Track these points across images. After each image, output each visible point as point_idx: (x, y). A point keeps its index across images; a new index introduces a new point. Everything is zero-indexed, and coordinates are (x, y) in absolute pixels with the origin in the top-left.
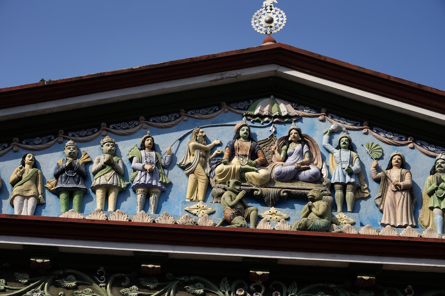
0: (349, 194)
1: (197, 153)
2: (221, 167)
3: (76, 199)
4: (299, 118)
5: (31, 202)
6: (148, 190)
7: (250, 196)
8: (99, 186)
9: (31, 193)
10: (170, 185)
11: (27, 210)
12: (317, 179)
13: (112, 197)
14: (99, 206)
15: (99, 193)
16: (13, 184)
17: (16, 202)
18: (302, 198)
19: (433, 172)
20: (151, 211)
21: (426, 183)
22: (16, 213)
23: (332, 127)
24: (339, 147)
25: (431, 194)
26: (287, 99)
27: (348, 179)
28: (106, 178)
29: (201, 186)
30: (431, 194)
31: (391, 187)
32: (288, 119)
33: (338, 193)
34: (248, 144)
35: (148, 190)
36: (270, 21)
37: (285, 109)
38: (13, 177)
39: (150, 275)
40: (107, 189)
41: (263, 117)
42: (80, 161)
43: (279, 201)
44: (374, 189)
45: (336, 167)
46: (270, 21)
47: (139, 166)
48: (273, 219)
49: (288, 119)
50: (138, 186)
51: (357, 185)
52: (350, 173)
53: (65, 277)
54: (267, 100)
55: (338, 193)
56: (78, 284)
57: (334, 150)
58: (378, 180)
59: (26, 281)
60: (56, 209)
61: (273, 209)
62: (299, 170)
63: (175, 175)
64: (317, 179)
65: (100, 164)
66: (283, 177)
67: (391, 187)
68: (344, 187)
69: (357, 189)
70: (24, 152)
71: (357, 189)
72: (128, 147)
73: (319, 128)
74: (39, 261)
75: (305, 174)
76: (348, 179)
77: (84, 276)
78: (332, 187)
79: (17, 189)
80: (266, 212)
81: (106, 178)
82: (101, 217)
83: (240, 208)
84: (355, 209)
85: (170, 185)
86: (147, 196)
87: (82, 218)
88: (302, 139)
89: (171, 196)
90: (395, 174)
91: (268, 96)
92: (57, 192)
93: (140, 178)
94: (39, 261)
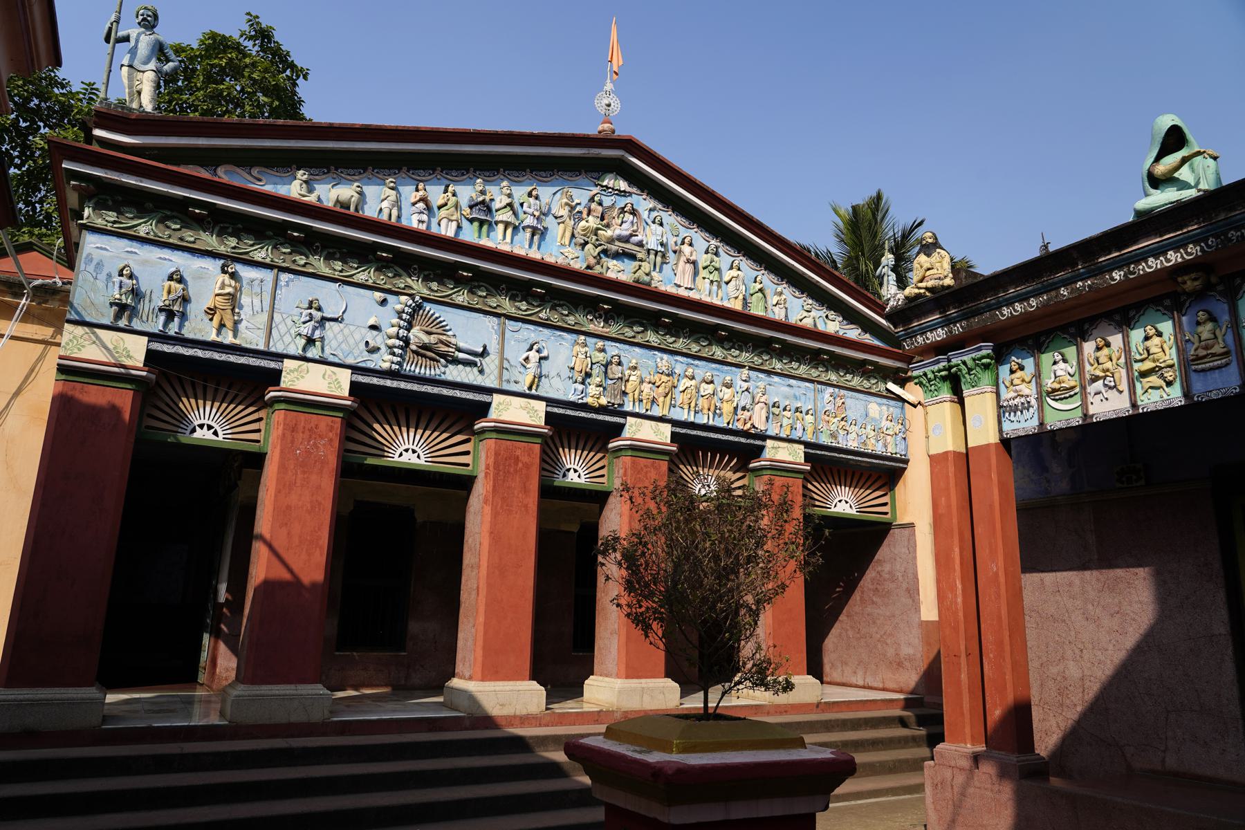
0: (659, 259)
1: (567, 208)
2: (583, 223)
3: (485, 228)
4: (630, 194)
5: (454, 224)
6: (534, 230)
7: (605, 252)
8: (501, 222)
9: (454, 218)
10: (546, 229)
11: (448, 230)
12: (640, 244)
13: (509, 231)
14: (500, 236)
15: (501, 227)
16: (440, 208)
17: (444, 222)
18: (633, 257)
19: (707, 252)
20: (535, 247)
21: (703, 260)
22: (443, 233)
23: (651, 206)
24: (654, 222)
25: (704, 268)
26: (626, 179)
27: (660, 248)
28: (506, 216)
29: (568, 234)
30: (704, 268)
31: (683, 259)
32: (623, 194)
33: (652, 256)
34: (600, 209)
35: (534, 230)
36: (609, 105)
37: (623, 185)
38: (441, 202)
40: (507, 224)
41: (608, 188)
42: (488, 198)
43: (617, 256)
44: (671, 257)
45: (652, 237)
46: (609, 105)
47: (530, 211)
48: (618, 270)
49: (623, 194)
50: (528, 227)
51: (662, 254)
52: (662, 244)
53: (479, 287)
54: (611, 175)
55: (652, 256)
57: (658, 227)
58: (675, 252)
60: (470, 235)
61: (615, 262)
62: (631, 235)
63: (549, 222)
64: (640, 244)
65: (504, 204)
66: (621, 239)
67: (683, 259)
68: (657, 252)
69: (664, 256)
70: (447, 182)
71: (664, 256)
72: (520, 192)
73: (644, 204)
75: (634, 239)
76: (660, 248)
78: (649, 251)
79: (443, 212)
80: (612, 263)
81: (506, 216)
83: (598, 258)
84: (660, 271)
85: (546, 229)
86: (533, 235)
88: (634, 212)
89: (548, 237)
90: (686, 249)
91: (611, 172)
92: (471, 221)
93: (529, 221)
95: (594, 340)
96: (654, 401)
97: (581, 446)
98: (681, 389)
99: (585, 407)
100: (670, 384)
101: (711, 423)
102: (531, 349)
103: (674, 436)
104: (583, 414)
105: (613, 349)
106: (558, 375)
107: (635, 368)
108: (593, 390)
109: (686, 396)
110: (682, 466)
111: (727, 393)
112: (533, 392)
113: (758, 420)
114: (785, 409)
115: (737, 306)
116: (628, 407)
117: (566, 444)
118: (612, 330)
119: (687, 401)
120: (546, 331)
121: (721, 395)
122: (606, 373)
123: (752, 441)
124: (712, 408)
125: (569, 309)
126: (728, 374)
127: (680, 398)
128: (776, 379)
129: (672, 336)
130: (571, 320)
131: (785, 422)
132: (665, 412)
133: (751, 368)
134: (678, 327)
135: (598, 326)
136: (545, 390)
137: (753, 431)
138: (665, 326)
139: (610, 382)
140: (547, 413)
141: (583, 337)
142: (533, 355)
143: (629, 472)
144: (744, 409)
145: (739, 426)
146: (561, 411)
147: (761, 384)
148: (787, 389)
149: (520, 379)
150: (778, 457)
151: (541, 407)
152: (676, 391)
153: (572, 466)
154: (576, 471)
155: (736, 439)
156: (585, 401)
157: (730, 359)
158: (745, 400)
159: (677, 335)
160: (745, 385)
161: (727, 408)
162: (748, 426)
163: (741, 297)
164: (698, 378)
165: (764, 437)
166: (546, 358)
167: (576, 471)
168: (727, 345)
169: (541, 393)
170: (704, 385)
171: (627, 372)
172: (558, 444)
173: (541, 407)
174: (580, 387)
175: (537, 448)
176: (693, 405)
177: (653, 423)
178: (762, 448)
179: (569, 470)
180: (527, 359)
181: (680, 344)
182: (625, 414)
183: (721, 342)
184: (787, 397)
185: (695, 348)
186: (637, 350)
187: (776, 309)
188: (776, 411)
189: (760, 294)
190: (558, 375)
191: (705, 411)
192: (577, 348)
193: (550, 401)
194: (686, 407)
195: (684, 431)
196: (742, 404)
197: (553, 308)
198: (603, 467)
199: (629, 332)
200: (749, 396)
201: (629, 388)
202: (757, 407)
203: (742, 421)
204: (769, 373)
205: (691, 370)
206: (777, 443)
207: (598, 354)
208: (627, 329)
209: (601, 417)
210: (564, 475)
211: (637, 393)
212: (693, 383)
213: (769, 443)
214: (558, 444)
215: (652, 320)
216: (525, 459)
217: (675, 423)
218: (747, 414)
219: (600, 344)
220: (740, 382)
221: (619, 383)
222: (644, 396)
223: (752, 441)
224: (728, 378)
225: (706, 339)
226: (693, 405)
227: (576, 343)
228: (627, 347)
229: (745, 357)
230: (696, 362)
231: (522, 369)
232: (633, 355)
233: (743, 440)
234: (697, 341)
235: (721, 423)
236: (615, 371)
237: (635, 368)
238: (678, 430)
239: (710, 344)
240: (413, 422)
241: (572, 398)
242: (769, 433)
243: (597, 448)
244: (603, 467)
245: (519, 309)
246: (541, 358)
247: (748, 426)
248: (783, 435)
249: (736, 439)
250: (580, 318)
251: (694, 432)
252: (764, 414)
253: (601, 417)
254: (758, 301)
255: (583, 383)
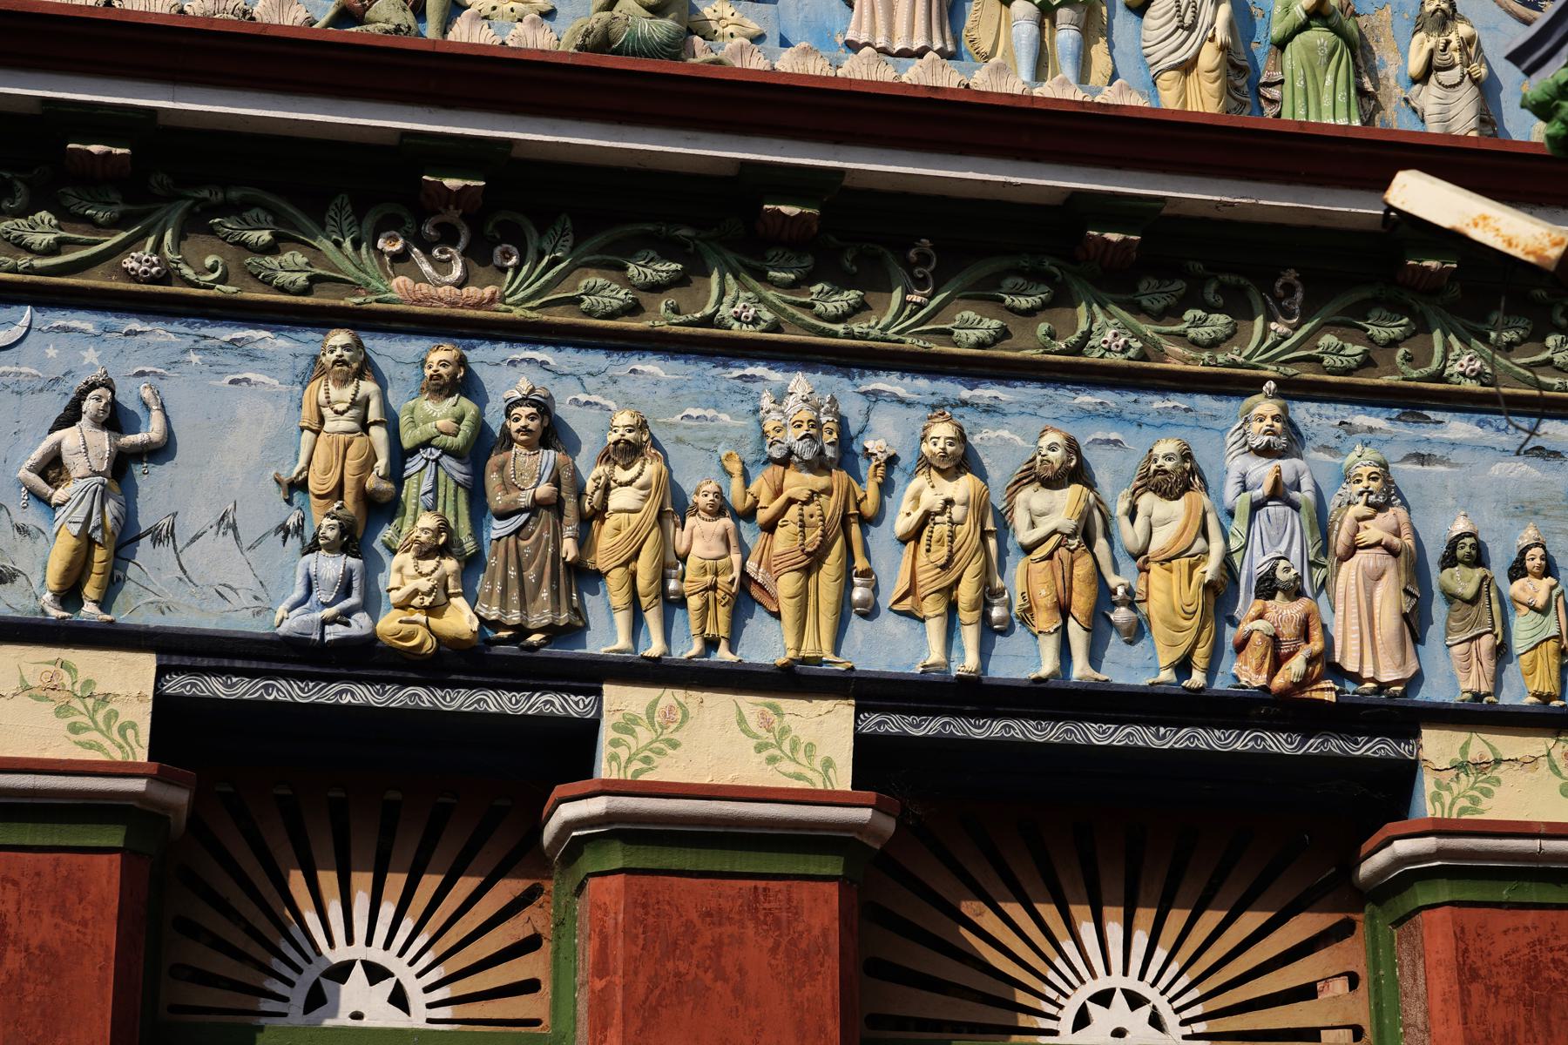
39: (95, 178)
56: (277, 237)
59: (266, 236)
74: (1114, 237)
77: (284, 205)
82: (1074, 94)
87: (497, 43)
94: (1114, 237)
95: (414, 347)
96: (746, 598)
97: (406, 849)
98: (903, 522)
99: (365, 659)
100: (831, 505)
101: (1080, 669)
102: (70, 417)
103: (871, 756)
104: (363, 695)
105: (509, 375)
106: (227, 524)
107: (628, 452)
108: (404, 574)
109: (929, 558)
110: (971, 908)
111: (1168, 519)
112: (90, 611)
113: (1363, 629)
114: (1518, 570)
115: (1202, 97)
116: (608, 635)
117: (323, 846)
118: (512, 291)
119: (928, 578)
120: (163, 334)
121: (1130, 534)
122: (476, 493)
123: (1335, 746)
124: (1081, 602)
125: (278, 218)
126: (1160, 431)
127: (895, 570)
128: (1458, 427)
129: (841, 282)
130: (291, 266)
131: (1524, 629)
132: (818, 643)
133: (1290, 390)
134: (861, 238)
135: (438, 282)
136: (159, 593)
137: (1326, 692)
138: (792, 240)
139: (498, 528)
140: (162, 704)
141: (340, 338)
142: (86, 446)
143: (618, 949)
144: (1267, 587)
145: (1247, 672)
146: (244, 689)
147: (1361, 460)
148: (1526, 470)
149: (22, 557)
150: (1496, 809)
151: (131, 679)
152: (880, 538)
153: (358, 951)
154: (376, 973)
155: (1241, 742)
156: (360, 625)
157: (1177, 359)
158: (1274, 544)
159: (871, 280)
160: (1263, 472)
161: (1168, 595)
162: (1295, 667)
163: (1209, 57)
164: (1000, 471)
165: (1402, 715)
166: (160, 452)
167: (376, 973)
168: (1152, 293)
169: (132, 611)
170: (1033, 497)
171: (592, 475)
172: (282, 850)
173: (131, 679)
174: (330, 566)
175: (105, 874)
176: (967, 592)
177: (751, 705)
178: (1404, 775)
179: (341, 972)
180: (52, 467)
181: (889, 317)
182: (593, 675)
183: (1117, 282)
184: (1526, 510)
185: (972, 327)
186: (652, 367)
187: (1429, 98)
188: (1464, 580)
189: (1319, 37)
190: (227, 524)
191: (1045, 620)
192: (318, 390)
193: (176, 649)
194: (932, 608)
195: (930, 727)
196: (1254, 564)
197: (195, 224)
198: (530, 944)
199: (602, 292)
200: (1295, 521)
201: (608, 543)
202: (1349, 575)
203: (1254, 652)
204: (1412, 402)
205: (943, 429)
206: (1479, 744)
207: (427, 406)
208: (594, 279)
209: (459, 701)
210: (316, 999)
211: (645, 567)
212: (964, 487)
213: (1436, 746)
214: (282, 850)
215: (714, 222)
216: (43, 930)
217: (869, 692)
218: (1285, 611)
219: (440, 355)
220: (1239, 463)
221: (542, 528)
222: (692, 579)
223: (1335, 746)
224: (1166, 447)
225: (1036, 277)
226: (967, 592)
227: (316, 368)
228: (596, 359)
229: (1266, 338)
230: (987, 392)
231: (32, 516)
232: (607, 397)
233: (1279, 744)
234: (984, 294)
235: (1139, 667)
236: (526, 473)
237: (628, 452)
238: (895, 724)
239: (1062, 299)
240: (364, 844)
241: (291, 622)
242: (1431, 693)
243: (490, 856)
244: (530, 944)
245: (22, 247)
246: (122, 465)
247: (1295, 667)
248: (1518, 693)
249: (1241, 742)
250: (338, 252)
251: (993, 729)
252: (1388, 602)
253: (459, 701)
254: (1312, 75)
255: (351, 540)
